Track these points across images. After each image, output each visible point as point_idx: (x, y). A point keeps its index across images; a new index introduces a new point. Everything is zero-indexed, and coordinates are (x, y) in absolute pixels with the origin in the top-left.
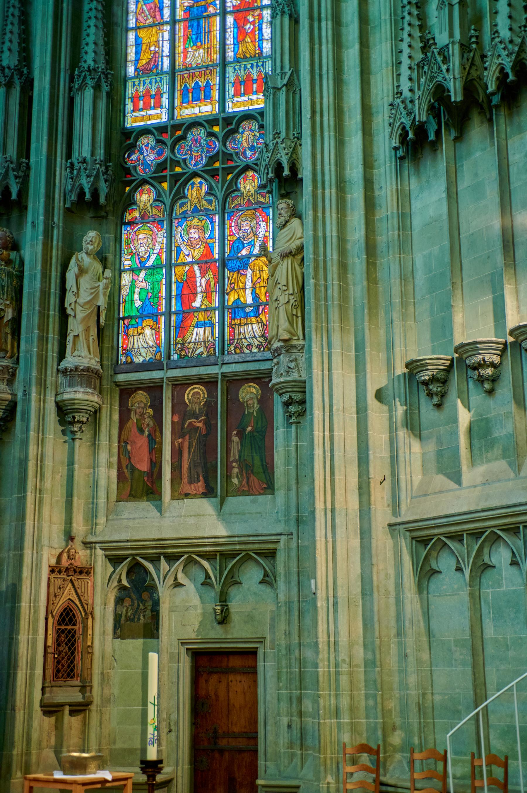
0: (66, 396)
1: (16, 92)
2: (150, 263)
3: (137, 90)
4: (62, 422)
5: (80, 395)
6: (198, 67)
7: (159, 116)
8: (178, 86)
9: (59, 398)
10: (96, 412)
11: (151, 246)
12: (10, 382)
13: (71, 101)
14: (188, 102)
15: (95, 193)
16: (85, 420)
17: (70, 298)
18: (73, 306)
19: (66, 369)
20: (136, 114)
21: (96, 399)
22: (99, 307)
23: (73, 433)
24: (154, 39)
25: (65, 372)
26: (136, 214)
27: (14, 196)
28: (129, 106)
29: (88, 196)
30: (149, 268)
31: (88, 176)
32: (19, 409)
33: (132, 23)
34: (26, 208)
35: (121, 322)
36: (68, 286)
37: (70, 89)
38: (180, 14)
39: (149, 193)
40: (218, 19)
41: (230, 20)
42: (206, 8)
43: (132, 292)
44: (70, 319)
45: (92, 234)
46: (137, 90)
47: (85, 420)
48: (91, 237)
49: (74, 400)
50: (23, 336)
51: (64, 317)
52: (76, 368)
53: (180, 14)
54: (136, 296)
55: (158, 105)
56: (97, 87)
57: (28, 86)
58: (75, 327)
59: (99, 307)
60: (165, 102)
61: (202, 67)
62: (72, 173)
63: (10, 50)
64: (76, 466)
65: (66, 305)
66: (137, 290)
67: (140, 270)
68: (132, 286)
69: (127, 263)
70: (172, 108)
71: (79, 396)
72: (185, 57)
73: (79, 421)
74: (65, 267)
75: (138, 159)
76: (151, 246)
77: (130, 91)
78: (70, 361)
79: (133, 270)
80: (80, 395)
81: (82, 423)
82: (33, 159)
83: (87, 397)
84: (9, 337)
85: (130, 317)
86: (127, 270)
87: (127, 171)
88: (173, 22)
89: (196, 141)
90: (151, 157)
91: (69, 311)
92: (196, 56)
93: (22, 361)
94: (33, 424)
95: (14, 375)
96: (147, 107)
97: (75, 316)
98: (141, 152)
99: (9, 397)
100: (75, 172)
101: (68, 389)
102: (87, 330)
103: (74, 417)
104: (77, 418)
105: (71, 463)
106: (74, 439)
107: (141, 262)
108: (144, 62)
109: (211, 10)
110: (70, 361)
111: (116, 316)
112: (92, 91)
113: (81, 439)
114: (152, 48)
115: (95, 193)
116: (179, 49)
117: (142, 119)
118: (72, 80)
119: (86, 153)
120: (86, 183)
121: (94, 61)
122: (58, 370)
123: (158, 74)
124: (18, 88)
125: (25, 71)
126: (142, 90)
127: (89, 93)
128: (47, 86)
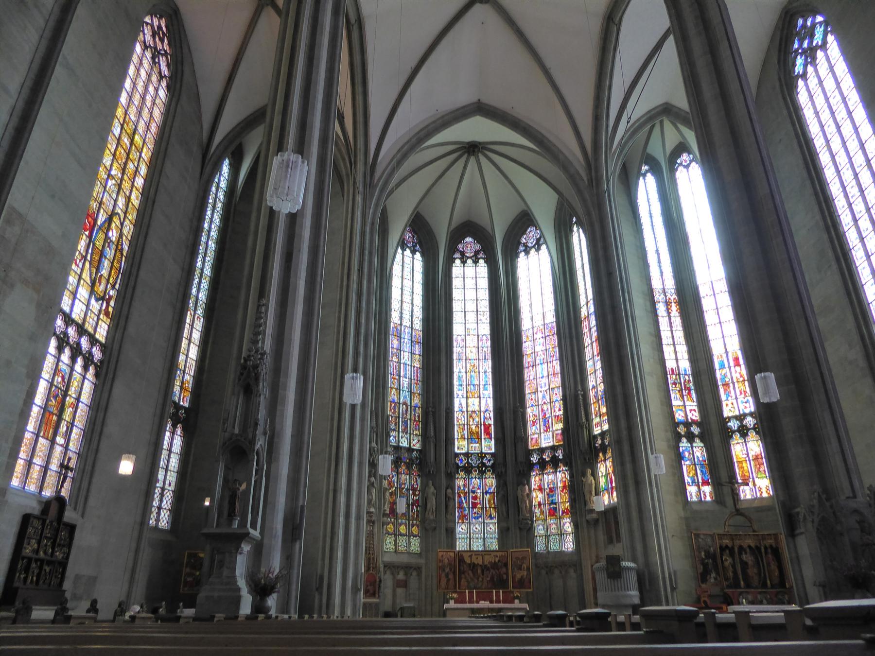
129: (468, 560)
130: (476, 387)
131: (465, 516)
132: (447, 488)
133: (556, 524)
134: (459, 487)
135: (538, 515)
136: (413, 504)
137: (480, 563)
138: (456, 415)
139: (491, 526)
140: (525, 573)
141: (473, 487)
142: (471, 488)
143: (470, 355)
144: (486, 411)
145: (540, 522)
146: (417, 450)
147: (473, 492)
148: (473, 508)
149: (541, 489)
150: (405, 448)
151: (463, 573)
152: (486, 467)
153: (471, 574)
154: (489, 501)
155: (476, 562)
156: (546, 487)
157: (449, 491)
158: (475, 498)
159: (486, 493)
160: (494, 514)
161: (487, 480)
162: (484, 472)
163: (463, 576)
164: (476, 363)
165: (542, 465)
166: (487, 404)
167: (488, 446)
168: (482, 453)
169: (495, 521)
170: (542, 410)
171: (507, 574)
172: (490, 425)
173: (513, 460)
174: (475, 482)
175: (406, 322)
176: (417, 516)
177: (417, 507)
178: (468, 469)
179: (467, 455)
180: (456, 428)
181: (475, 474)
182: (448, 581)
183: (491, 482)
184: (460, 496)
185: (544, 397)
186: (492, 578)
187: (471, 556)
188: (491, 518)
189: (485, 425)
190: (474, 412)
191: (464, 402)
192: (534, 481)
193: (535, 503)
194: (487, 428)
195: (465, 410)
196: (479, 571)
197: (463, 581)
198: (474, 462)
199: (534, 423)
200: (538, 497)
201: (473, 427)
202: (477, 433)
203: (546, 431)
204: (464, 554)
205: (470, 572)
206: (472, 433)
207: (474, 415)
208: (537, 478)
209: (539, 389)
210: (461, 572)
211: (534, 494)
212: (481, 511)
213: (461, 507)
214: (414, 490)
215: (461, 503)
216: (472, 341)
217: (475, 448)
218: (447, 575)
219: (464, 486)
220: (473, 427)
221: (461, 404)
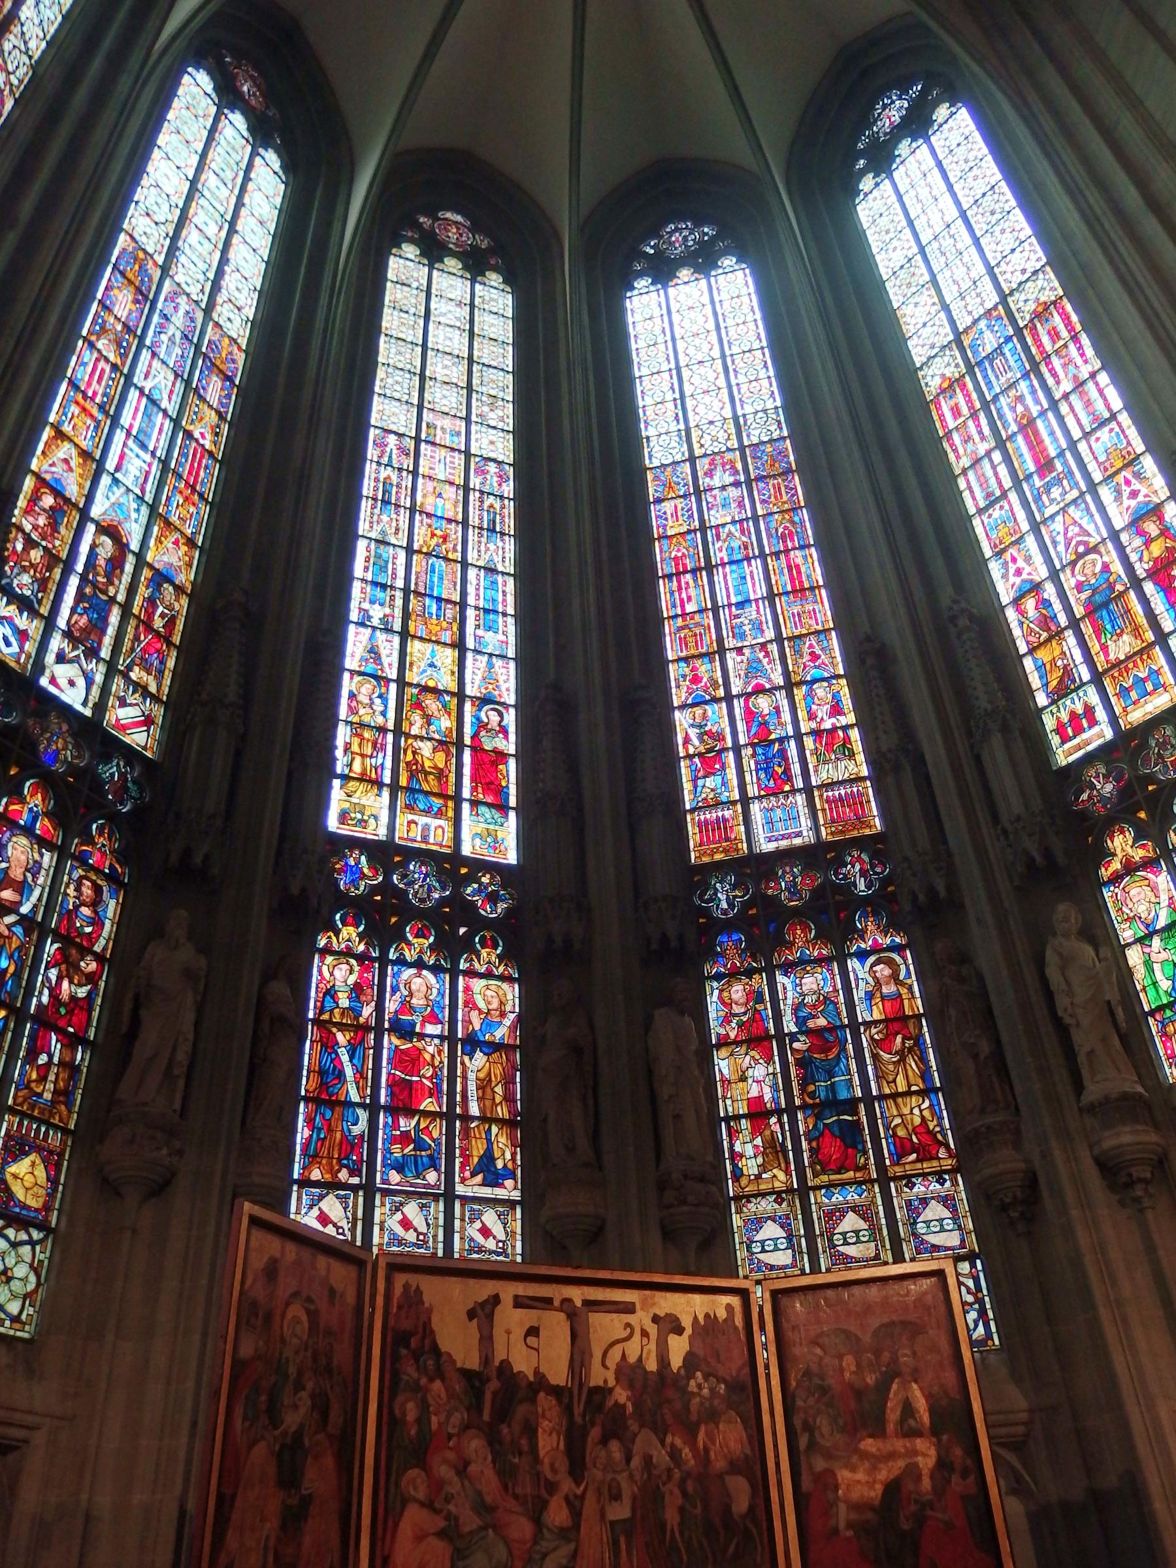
0: (1108, 1144)
1: (908, 773)
2: (1161, 923)
3: (1058, 718)
4: (1113, 1187)
5: (1126, 1137)
6: (1128, 658)
7: (1101, 735)
8: (1110, 690)
9: (1096, 1151)
10: (1161, 1162)
11: (1153, 900)
12: (1017, 1145)
13: (978, 758)
14: (1134, 703)
15: (1047, 853)
16: (1148, 1175)
17: (1062, 1002)
18: (1070, 1011)
19: (1092, 1104)
20: (1068, 746)
21: (1153, 1138)
22: (1109, 1002)
23: (1137, 1200)
24: (1057, 652)
25: (1091, 1109)
26: (1116, 865)
27: (943, 893)
28: (1055, 740)
29: (1039, 859)
30: (1163, 930)
31: (1030, 835)
32: (1042, 1180)
33: (1023, 648)
34: (962, 906)
35: (1151, 1021)
36: (1053, 987)
37: (972, 747)
38: (1079, 611)
39: (1122, 832)
40: (1132, 593)
41: (1149, 588)
42: (1112, 587)
43: (1151, 971)
44: (1073, 1031)
45: (1061, 908)
46: (1058, 718)
47: (1148, 1175)
48: (1066, 913)
49: (1120, 1146)
50: (1013, 1074)
51: (1063, 1031)
52: (1107, 1099)
53: (1079, 611)
54: (1159, 975)
55: (1093, 722)
56: (1005, 729)
57: (919, 761)
58: (1083, 1041)
59: (1109, 1002)
60: (1101, 714)
61: (1135, 654)
62: (1007, 838)
63: (885, 732)
64: (1161, 1253)
65: (1060, 1013)
66: (1157, 967)
67: (1150, 936)
68: (1148, 964)
69: (1127, 934)
70: (1113, 720)
71: (1127, 1139)
72: (1106, 654)
73: (1140, 1180)
74: (1040, 963)
75: (1090, 797)
76: (1153, 900)
77: (1049, 723)
78: (1093, 1091)
79: (1139, 940)
80: (1126, 1137)
81: (1147, 1182)
82: (952, 841)
83: (1139, 1138)
84: (995, 1079)
85: (1161, 1008)
86: (1129, 945)
87: (1083, 816)
88: (1074, 623)
89: (1165, 743)
90: (1109, 787)
91: (1068, 1020)
92: (1122, 647)
93: (1023, 1108)
94: (1070, 1195)
95: (1017, 1132)
96: (1079, 730)
97: (1078, 1025)
98: (1092, 787)
99: (1023, 1166)
100: (1011, 837)
101: (1107, 1134)
102: (1104, 1039)
103: (1130, 1175)
104: (1135, 1175)
105: (1150, 1249)
106: (1141, 1211)
107: (1147, 926)
108: (1055, 683)
109: (1119, 587)
110: (1093, 1091)
111: (1138, 1011)
112: (999, 735)
113: (1153, 1208)
114: (1059, 663)
115: (1047, 853)
116: (1095, 647)
117: (1079, 747)
118: (970, 734)
119: (1017, 807)
120: (1032, 846)
121: (990, 702)
122: (1080, 1110)
123: (1079, 688)
124: (909, 769)
125: (910, 747)
126: (1065, 717)
127: (997, 740)
128: (942, 752)
129: (458, 1343)
130: (450, 612)
131: (349, 1145)
132: (268, 977)
133: (863, 1212)
134: (331, 993)
135: (751, 1167)
136: (45, 1021)
137: (558, 1375)
138: (347, 684)
139: (490, 1218)
140: (926, 1455)
141: (406, 1006)
142: (391, 1006)
143: (428, 502)
144: (484, 701)
145: (766, 1205)
146: (131, 754)
147: (404, 1031)
148: (394, 1110)
149: (756, 1039)
150: (66, 710)
151: (421, 1453)
152: (477, 923)
153: (483, 1469)
154: (484, 1085)
155: (522, 1363)
156: (790, 1026)
157: (279, 988)
158: (409, 1061)
159: (472, 1043)
160: (505, 1152)
161: (478, 985)
162: (467, 945)
163: (415, 1482)
164: (455, 532)
165: (765, 935)
166: (489, 677)
167: (493, 836)
168: (456, 857)
169: (510, 1190)
170: (750, 715)
171: (753, 1466)
172: (501, 756)
173: (612, 911)
174: (422, 986)
175: (191, 272)
176: (63, 1095)
177: (71, 1042)
178: (384, 918)
179: (385, 853)
180: (343, 734)
181: (418, 945)
182: (294, 1518)
183: (493, 998)
184: (328, 1044)
185: (753, 669)
186: (650, 1498)
187: (484, 1312)
188: (494, 1179)
189: (477, 748)
190: (435, 691)
191: (389, 647)
192: (723, 1004)
193: (733, 1103)
194: (488, 764)
195: (393, 674)
196: (549, 1443)
197: (413, 1518)
198: (422, 886)
199: (710, 761)
200: (747, 1079)
201: (426, 748)
202: (441, 774)
203: (774, 793)
204: (432, 1289)
205: (475, 1445)
206: (416, 769)
207: (432, 704)
208: (738, 991)
209: (730, 643)
210: (407, 1449)
211: (723, 1065)
212: (438, 1130)
213: (327, 1098)
214: (74, 946)
215: (330, 1075)
216: (439, 464)
217: (426, 829)
218: (289, 1474)
219: (357, 990)
220: (426, 748)
221: (374, 652)
